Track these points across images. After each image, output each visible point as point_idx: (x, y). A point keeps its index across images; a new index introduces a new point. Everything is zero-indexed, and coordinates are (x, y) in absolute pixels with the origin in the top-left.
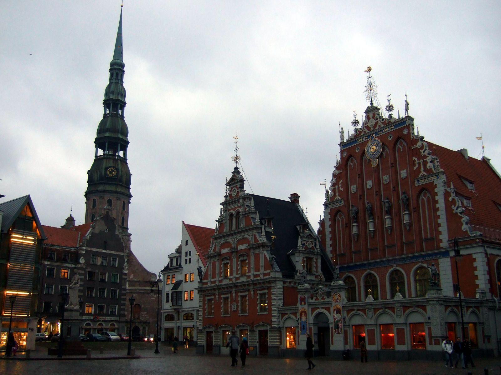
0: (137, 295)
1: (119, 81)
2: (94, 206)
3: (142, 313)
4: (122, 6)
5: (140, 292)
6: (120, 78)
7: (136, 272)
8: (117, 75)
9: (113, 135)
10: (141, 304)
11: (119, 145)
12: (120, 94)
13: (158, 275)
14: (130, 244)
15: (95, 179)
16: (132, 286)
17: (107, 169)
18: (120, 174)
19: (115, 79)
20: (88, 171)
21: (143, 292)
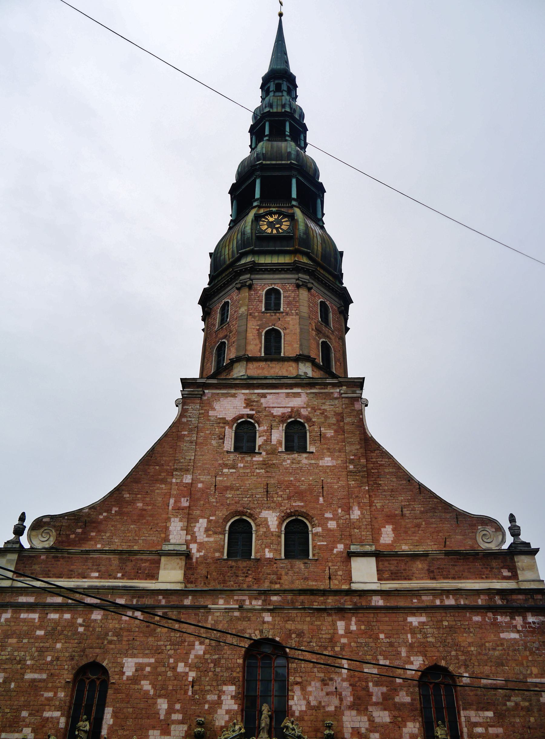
0: (423, 619)
1: (285, 94)
2: (223, 321)
3: (468, 718)
4: (281, 15)
5: (438, 602)
6: (284, 87)
7: (403, 515)
8: (278, 88)
9: (274, 162)
10: (451, 668)
11: (294, 181)
12: (288, 106)
13: (506, 525)
14: (361, 412)
15: (227, 257)
16: (395, 576)
17: (258, 218)
18: (301, 227)
19: (274, 92)
20: (211, 254)
21: (450, 601)
